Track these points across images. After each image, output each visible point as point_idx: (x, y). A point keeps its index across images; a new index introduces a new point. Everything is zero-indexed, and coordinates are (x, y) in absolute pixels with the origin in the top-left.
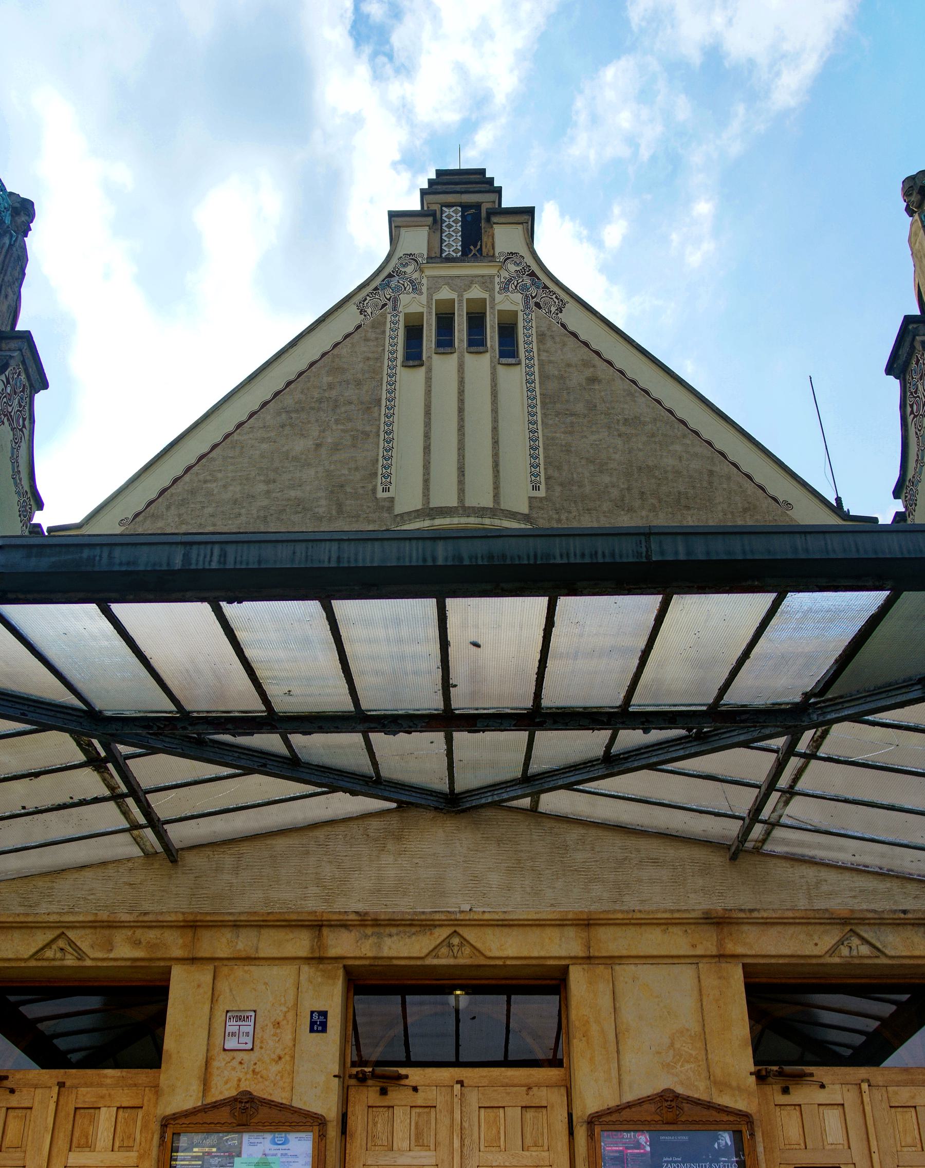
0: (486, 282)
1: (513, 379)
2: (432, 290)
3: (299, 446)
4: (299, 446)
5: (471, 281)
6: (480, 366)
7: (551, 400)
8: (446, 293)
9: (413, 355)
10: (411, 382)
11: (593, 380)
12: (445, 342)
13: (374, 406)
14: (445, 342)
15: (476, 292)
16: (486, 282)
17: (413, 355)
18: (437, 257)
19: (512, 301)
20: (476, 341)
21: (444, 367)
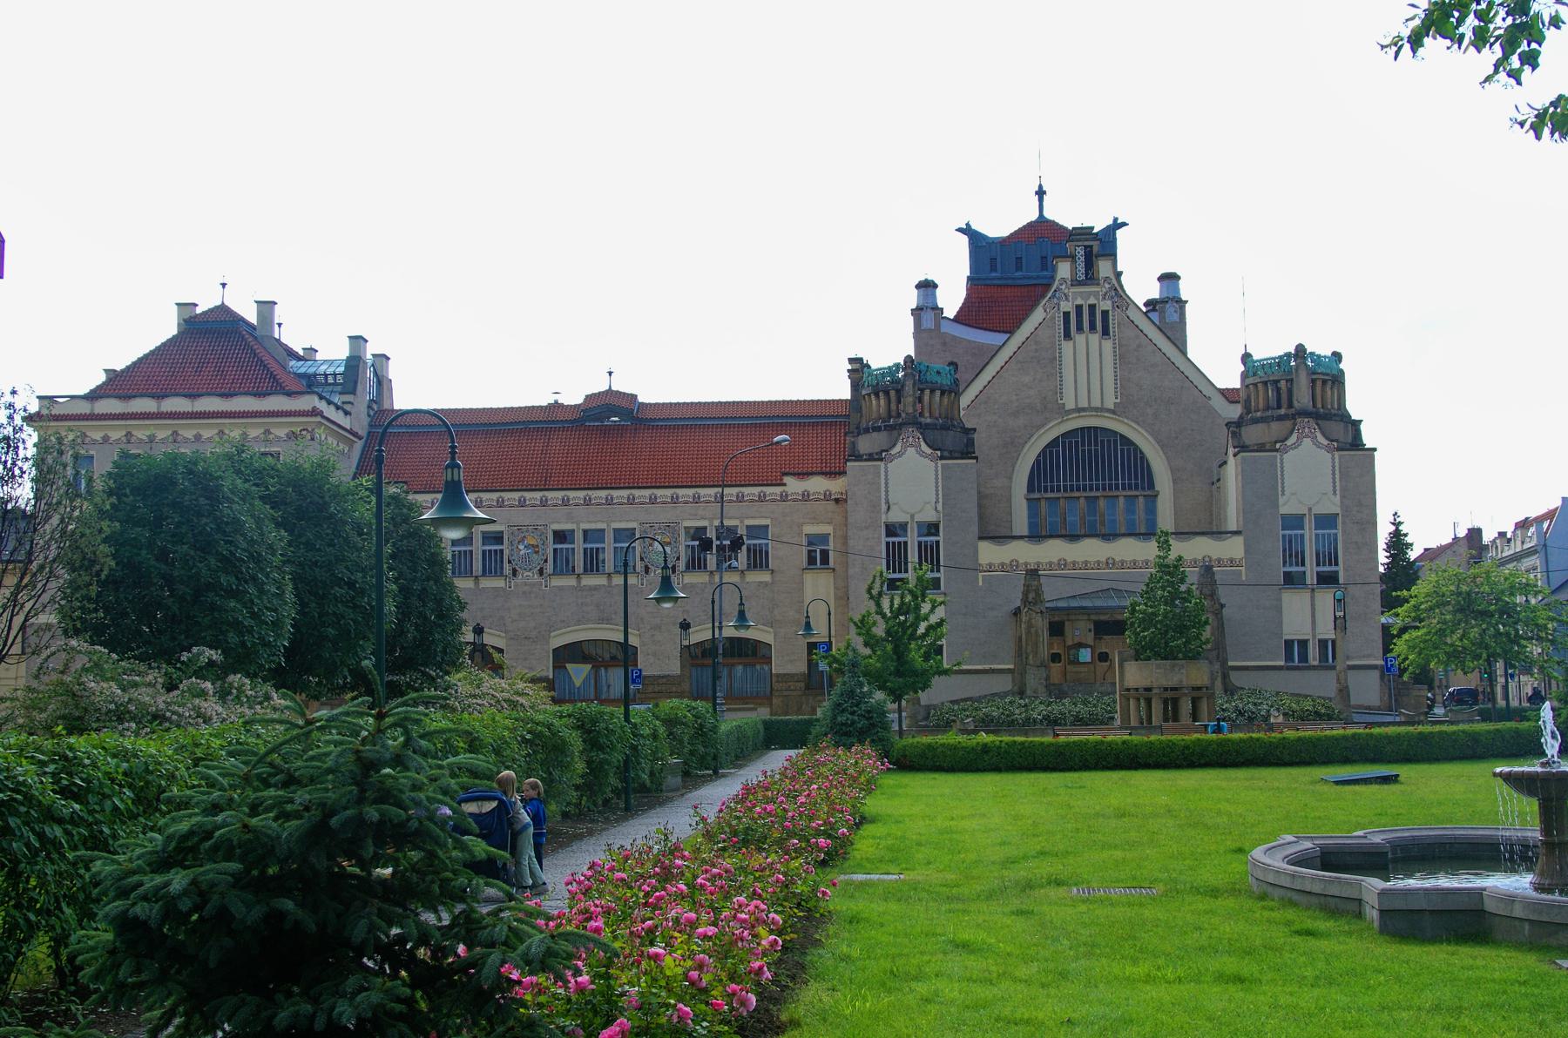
0: (1096, 294)
1: (1108, 345)
2: (1074, 299)
3: (1027, 379)
4: (1027, 379)
5: (1090, 294)
6: (1095, 338)
7: (1121, 358)
8: (1079, 301)
9: (1067, 336)
10: (1067, 347)
11: (1139, 346)
12: (1080, 329)
13: (1055, 361)
14: (1080, 329)
15: (1092, 301)
16: (1096, 294)
17: (1067, 336)
18: (1076, 283)
19: (1106, 305)
20: (1093, 327)
21: (1080, 339)
